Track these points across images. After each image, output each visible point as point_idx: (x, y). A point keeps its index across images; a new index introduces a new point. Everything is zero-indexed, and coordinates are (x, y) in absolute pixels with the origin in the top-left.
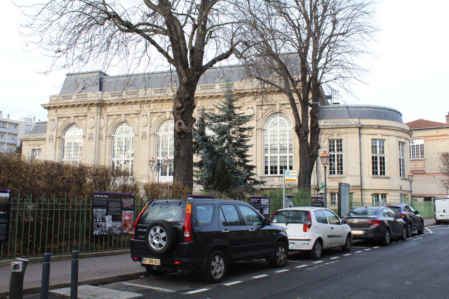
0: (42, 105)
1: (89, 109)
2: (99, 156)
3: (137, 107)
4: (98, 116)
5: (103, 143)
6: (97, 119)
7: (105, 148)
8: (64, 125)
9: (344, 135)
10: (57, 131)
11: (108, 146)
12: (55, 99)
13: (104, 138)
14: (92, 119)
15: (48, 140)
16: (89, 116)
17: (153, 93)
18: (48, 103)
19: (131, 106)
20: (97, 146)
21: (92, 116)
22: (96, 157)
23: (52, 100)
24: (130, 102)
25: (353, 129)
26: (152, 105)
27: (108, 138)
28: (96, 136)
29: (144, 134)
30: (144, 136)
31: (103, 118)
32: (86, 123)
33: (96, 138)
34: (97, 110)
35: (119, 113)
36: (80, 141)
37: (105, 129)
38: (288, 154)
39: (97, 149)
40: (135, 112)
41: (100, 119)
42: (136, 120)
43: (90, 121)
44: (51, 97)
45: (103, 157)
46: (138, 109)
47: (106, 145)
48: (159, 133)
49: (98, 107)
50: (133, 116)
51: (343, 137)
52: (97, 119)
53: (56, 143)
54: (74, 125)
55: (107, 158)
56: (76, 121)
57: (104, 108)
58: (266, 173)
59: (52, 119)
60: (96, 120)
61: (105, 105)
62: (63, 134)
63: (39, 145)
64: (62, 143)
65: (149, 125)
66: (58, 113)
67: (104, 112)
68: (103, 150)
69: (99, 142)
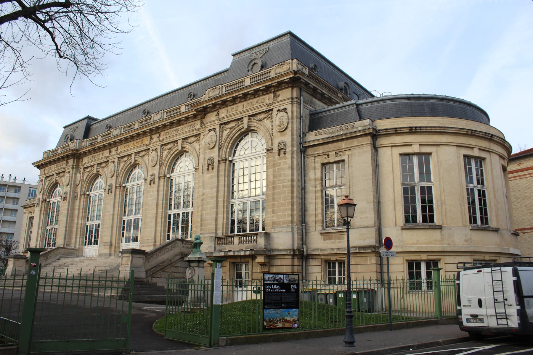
1: (276, 96)
14: (282, 114)
16: (275, 110)
64: (229, 171)
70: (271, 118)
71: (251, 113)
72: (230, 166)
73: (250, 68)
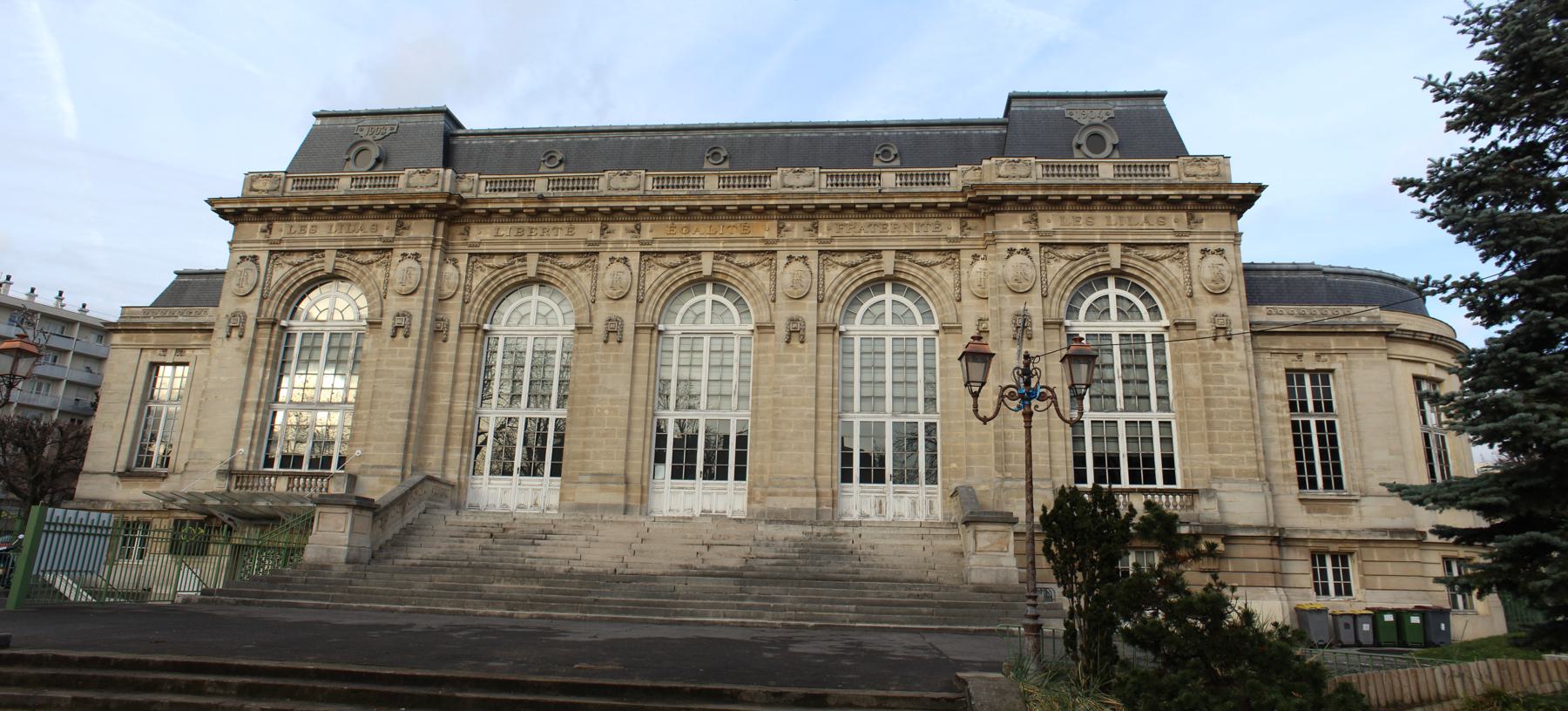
0: (210, 202)
1: (400, 227)
2: (429, 398)
3: (589, 231)
4: (437, 253)
5: (447, 352)
6: (431, 263)
7: (456, 369)
8: (293, 279)
9: (1339, 358)
10: (263, 298)
12: (268, 187)
13: (453, 332)
15: (220, 332)
16: (398, 252)
17: (649, 187)
18: (237, 192)
20: (423, 360)
21: (410, 251)
22: (418, 401)
23: (252, 189)
24: (564, 211)
25: (1366, 338)
26: (647, 227)
27: (468, 337)
28: (423, 322)
30: (614, 331)
31: (455, 262)
33: (422, 331)
34: (435, 233)
35: (520, 248)
37: (457, 301)
40: (582, 248)
41: (440, 265)
42: (583, 277)
43: (402, 270)
44: (252, 178)
45: (443, 400)
46: (595, 236)
47: (457, 359)
49: (438, 220)
50: (572, 261)
51: (1337, 364)
52: (431, 263)
53: (254, 341)
55: (460, 406)
56: (345, 265)
59: (247, 254)
60: (426, 267)
61: (467, 218)
62: (285, 310)
63: (180, 351)
64: (278, 345)
65: (633, 293)
66: (275, 236)
67: (458, 240)
68: (444, 377)
69: (431, 348)
71: (343, 245)
73: (352, 155)
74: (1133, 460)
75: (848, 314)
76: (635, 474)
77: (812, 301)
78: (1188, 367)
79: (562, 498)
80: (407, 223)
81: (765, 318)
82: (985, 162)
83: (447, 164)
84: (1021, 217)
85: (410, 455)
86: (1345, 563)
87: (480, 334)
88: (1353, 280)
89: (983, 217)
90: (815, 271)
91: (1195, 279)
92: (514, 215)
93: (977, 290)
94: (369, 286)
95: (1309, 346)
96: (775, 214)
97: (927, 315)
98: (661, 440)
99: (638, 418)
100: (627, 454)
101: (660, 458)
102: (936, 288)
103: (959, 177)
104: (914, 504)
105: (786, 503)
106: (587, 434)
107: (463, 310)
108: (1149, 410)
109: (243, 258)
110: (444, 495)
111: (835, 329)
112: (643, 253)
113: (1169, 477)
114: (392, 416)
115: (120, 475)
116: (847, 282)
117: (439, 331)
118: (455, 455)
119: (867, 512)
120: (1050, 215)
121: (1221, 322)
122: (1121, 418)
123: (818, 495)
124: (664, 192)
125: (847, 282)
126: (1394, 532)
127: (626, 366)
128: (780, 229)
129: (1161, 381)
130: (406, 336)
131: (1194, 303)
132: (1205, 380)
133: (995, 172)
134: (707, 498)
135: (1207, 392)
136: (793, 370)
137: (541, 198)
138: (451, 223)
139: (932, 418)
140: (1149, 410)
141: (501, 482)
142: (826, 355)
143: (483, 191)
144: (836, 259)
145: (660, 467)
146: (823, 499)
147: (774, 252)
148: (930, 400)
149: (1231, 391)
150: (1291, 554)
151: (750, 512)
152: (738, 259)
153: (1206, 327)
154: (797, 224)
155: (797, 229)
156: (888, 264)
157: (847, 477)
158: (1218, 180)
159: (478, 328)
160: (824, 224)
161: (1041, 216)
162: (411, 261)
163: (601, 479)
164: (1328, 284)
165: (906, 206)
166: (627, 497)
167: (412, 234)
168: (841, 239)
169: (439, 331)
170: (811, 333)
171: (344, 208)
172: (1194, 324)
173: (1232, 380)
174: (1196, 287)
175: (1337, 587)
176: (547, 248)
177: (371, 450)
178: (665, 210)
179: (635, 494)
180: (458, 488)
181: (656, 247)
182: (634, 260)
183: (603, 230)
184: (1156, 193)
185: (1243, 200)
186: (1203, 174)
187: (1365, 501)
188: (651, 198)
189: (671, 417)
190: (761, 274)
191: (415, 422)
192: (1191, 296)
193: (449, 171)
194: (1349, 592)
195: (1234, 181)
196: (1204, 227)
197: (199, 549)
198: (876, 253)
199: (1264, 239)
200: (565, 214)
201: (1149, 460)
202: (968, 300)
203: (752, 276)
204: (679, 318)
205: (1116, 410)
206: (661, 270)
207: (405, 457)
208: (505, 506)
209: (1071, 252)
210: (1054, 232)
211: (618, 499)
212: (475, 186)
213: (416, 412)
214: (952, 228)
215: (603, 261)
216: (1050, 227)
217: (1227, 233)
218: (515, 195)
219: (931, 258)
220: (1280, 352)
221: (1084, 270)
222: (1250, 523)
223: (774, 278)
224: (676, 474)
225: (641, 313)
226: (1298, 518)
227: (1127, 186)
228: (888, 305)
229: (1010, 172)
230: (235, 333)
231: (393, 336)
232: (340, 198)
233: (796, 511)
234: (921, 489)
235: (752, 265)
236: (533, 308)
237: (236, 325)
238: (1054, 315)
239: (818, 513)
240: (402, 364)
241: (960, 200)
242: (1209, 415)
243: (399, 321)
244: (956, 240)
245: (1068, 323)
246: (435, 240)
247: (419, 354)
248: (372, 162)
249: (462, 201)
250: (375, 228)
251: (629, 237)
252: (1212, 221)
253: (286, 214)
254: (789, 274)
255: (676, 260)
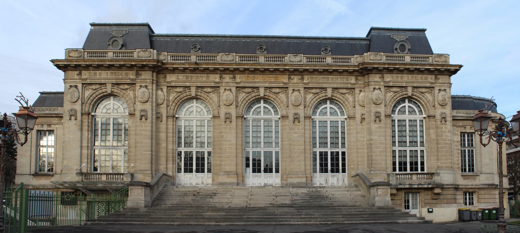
0: (52, 61)
2: (158, 144)
3: (215, 78)
4: (154, 85)
6: (152, 90)
7: (167, 133)
10: (82, 104)
11: (170, 130)
12: (76, 55)
13: (164, 118)
15: (66, 117)
16: (138, 85)
17: (237, 60)
18: (63, 57)
19: (206, 75)
20: (154, 129)
21: (143, 85)
22: (154, 145)
23: (69, 56)
27: (170, 120)
28: (152, 114)
29: (228, 116)
30: (228, 118)
31: (162, 90)
32: (135, 94)
33: (152, 117)
34: (152, 77)
35: (188, 84)
36: (126, 122)
37: (164, 105)
38: (419, 149)
39: (154, 133)
40: (213, 84)
41: (156, 91)
43: (141, 92)
44: (69, 51)
45: (163, 145)
46: (218, 80)
47: (167, 129)
48: (248, 116)
50: (209, 90)
52: (152, 90)
53: (82, 121)
54: (112, 98)
55: (170, 147)
56: (116, 90)
57: (161, 76)
58: (394, 169)
59: (73, 84)
60: (151, 91)
61: (165, 71)
62: (93, 109)
63: (49, 125)
64: (92, 123)
66: (83, 77)
67: (162, 80)
68: (163, 136)
69: (156, 124)
70: (134, 90)
71: (114, 81)
72: (92, 120)
73: (111, 43)
74: (411, 163)
75: (314, 113)
76: (239, 171)
77: (302, 107)
78: (432, 131)
79: (213, 180)
80: (140, 72)
81: (284, 113)
82: (365, 54)
83: (152, 47)
84: (378, 76)
85: (154, 166)
86: (472, 195)
87: (175, 119)
88: (481, 102)
89: (364, 76)
90: (303, 95)
91: (436, 100)
92: (184, 70)
93: (361, 103)
94: (127, 99)
95: (468, 124)
96: (287, 73)
97: (342, 113)
98: (248, 159)
99: (239, 151)
100: (237, 164)
101: (248, 165)
102: (346, 103)
103: (355, 60)
104: (338, 180)
105: (295, 181)
106: (220, 157)
107: (167, 109)
108: (417, 146)
109: (71, 86)
110: (168, 181)
111: (310, 117)
112: (237, 87)
113: (422, 169)
114: (144, 151)
115: (33, 175)
116: (314, 100)
117: (158, 118)
118: (170, 166)
119: (322, 183)
120: (388, 75)
121: (444, 116)
122: (408, 149)
123: (306, 177)
124: (243, 62)
125: (314, 100)
126: (489, 185)
127: (234, 131)
128: (289, 79)
129: (422, 137)
130: (146, 119)
131: (435, 109)
132: (437, 136)
133: (369, 57)
134: (266, 179)
135: (437, 140)
136: (296, 133)
137: (196, 63)
138: (158, 73)
139: (344, 150)
140: (417, 146)
141: (189, 175)
142: (307, 127)
143: (169, 59)
144: (310, 91)
145: (248, 169)
146: (308, 179)
147: (287, 88)
148: (343, 144)
149: (445, 140)
150: (459, 193)
151: (281, 184)
152: (274, 90)
153: (438, 117)
154: (295, 76)
155: (296, 79)
156: (329, 93)
157: (315, 171)
158: (445, 63)
159: (174, 116)
160: (306, 77)
161: (385, 75)
162: (143, 89)
163: (228, 173)
164: (474, 103)
165: (336, 71)
166: (238, 180)
167: (143, 77)
168: (313, 83)
169: (158, 118)
170: (302, 119)
171: (113, 66)
172: (434, 116)
173: (446, 136)
174: (436, 103)
175: (470, 203)
176: (199, 84)
177: (138, 164)
178: (245, 69)
179: (241, 178)
180: (173, 178)
181: (242, 85)
182: (234, 89)
183: (221, 77)
184: (426, 67)
185: (453, 70)
186: (441, 61)
187: (481, 175)
188: (240, 64)
189: (251, 150)
190: (282, 96)
191: (154, 153)
192: (434, 106)
193: (155, 51)
194: (473, 204)
195: (451, 63)
196: (440, 81)
197: (73, 203)
198: (325, 89)
199: (460, 85)
200: (206, 71)
201: (416, 163)
202: (358, 107)
203: (279, 97)
204: (251, 113)
205: (406, 146)
206: (244, 94)
207: (152, 167)
208: (191, 184)
209: (394, 89)
210: (390, 82)
211: (235, 180)
212: (166, 57)
213: (154, 149)
214: (352, 80)
215: (222, 90)
216: (388, 80)
217: (447, 83)
218: (183, 62)
219: (344, 91)
220: (459, 126)
221: (399, 97)
222: (448, 183)
223: (288, 98)
224: (254, 171)
225: (238, 111)
226: (462, 182)
227: (417, 65)
228: (328, 108)
229: (374, 58)
230: (73, 118)
231: (141, 119)
232: (111, 61)
233: (299, 183)
234: (341, 174)
235: (279, 93)
236: (194, 109)
237: (73, 114)
238: (388, 113)
239: (307, 183)
240: (146, 130)
241: (357, 68)
242: (438, 148)
243: (142, 113)
244: (354, 84)
245: (392, 115)
246: (153, 80)
247: (152, 127)
248: (120, 46)
249: (163, 64)
250: (127, 74)
251: (231, 81)
252: (442, 79)
253: (87, 67)
254: (293, 96)
255: (250, 90)
